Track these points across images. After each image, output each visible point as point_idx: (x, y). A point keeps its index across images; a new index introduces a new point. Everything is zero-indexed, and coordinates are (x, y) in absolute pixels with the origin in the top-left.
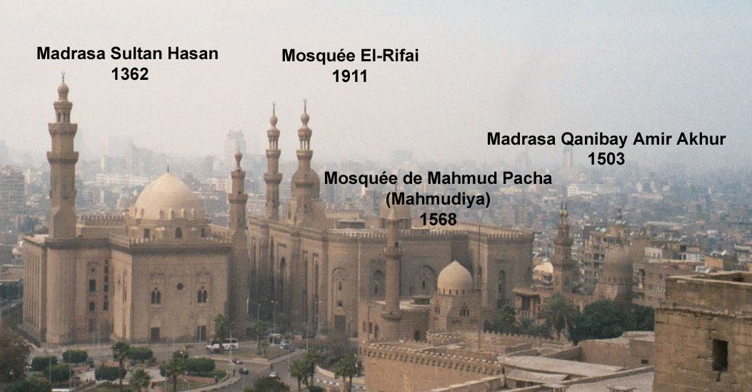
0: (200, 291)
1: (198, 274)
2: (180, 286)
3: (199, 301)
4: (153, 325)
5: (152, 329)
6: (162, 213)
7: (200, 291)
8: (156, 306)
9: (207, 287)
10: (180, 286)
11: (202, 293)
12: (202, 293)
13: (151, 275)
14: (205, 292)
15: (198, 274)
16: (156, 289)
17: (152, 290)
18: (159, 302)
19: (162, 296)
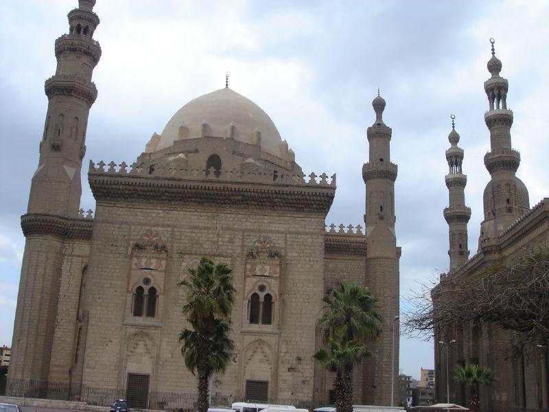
1: (251, 255)
3: (253, 320)
4: (133, 368)
5: (131, 376)
6: (183, 129)
7: (255, 296)
8: (142, 320)
9: (273, 287)
11: (262, 299)
12: (262, 299)
13: (137, 246)
14: (268, 297)
15: (251, 255)
16: (147, 281)
17: (137, 280)
18: (151, 313)
19: (161, 300)
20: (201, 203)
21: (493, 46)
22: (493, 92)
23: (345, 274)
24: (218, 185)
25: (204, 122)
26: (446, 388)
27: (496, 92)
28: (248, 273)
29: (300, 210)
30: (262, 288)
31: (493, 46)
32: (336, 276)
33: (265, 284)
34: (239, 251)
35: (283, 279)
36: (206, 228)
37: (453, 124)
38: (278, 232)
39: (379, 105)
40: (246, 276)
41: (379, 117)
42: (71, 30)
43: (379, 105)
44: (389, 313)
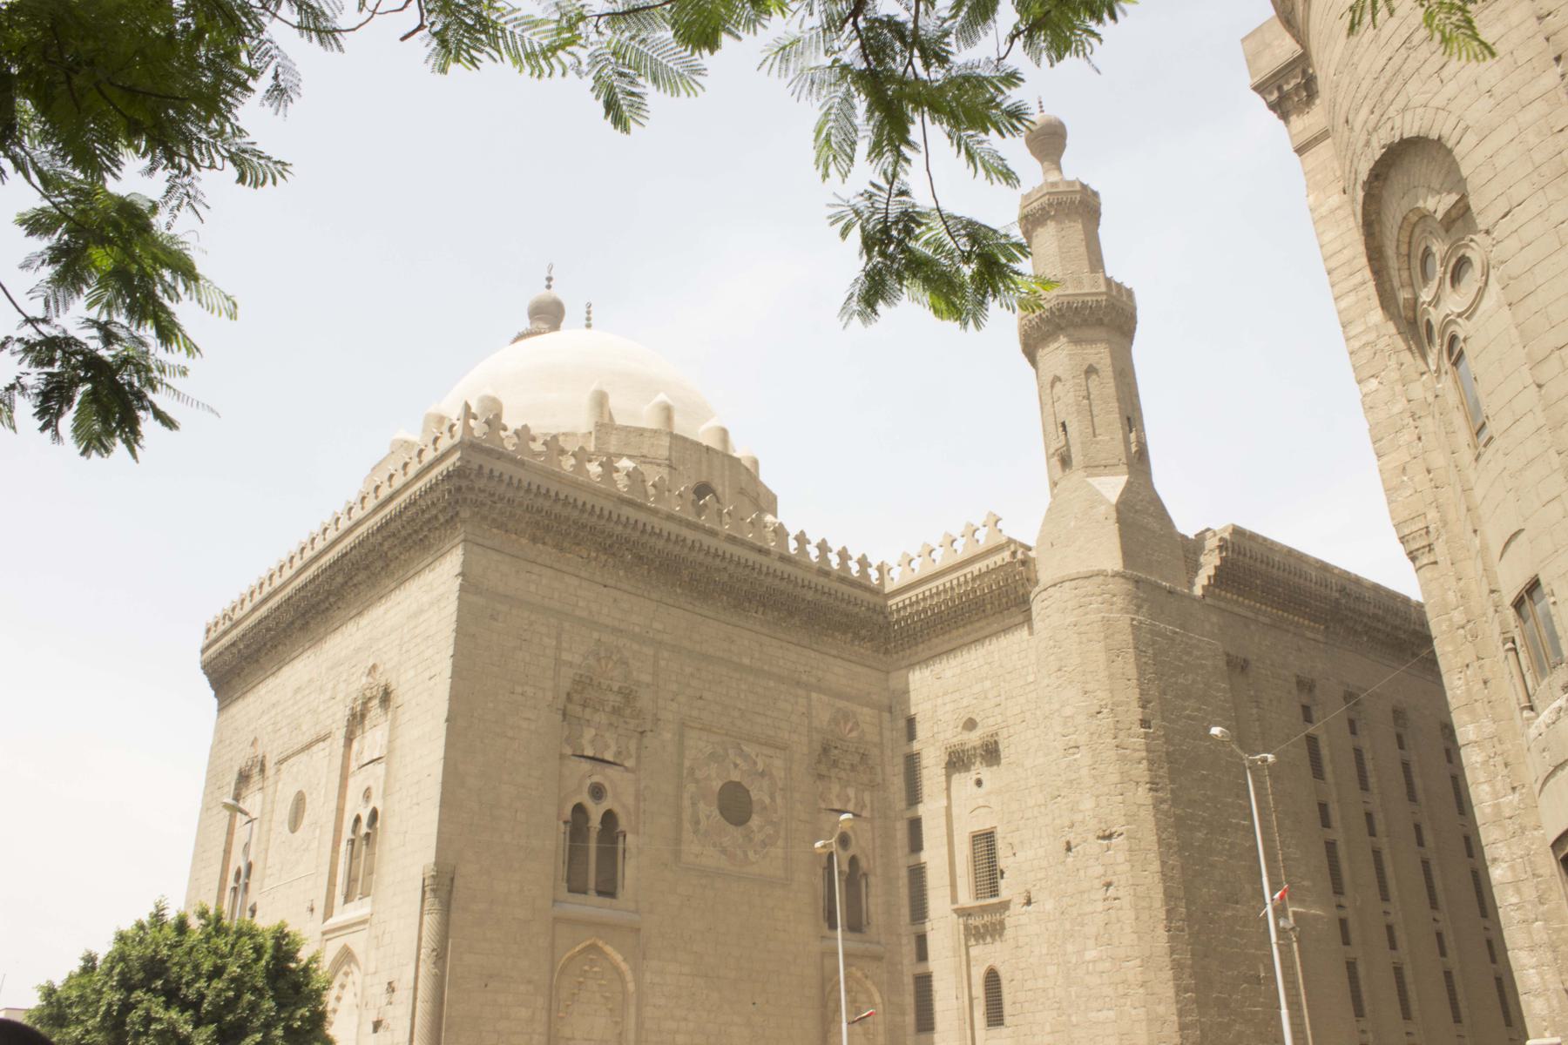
20: (305, 627)
23: (988, 684)
26: (1312, 1028)
32: (965, 703)
44: (1084, 772)
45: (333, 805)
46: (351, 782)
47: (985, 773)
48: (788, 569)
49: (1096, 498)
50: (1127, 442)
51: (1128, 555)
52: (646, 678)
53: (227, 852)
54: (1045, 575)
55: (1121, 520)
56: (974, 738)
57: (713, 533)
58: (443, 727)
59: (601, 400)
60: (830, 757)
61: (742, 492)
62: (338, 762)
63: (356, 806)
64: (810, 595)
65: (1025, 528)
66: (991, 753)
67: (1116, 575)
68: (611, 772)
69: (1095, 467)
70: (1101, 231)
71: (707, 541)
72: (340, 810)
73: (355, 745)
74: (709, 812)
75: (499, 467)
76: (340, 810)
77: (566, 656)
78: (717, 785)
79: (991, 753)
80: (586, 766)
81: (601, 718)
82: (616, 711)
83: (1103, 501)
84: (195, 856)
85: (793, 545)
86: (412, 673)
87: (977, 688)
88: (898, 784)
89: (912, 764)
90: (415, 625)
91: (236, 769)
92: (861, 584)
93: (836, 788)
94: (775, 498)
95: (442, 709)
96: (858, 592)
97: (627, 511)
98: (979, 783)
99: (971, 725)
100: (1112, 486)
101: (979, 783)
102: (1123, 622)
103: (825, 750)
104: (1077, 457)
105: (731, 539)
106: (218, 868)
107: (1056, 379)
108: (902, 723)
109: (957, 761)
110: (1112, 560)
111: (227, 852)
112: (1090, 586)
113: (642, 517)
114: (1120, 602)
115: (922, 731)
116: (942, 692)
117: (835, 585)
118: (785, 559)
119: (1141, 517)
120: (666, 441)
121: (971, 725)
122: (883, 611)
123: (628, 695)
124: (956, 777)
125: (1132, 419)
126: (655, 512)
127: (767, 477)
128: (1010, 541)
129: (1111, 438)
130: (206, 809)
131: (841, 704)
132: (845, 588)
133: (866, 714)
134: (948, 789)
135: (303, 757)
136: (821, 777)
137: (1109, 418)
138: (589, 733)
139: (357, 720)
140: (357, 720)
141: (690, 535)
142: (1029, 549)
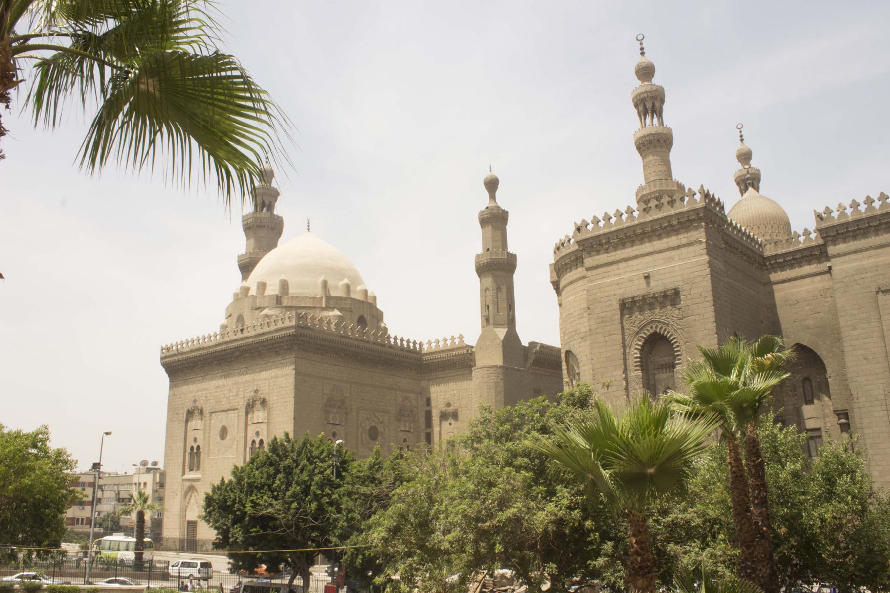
0: (253, 442)
2: (224, 433)
10: (224, 433)
17: (191, 442)
18: (198, 469)
20: (219, 364)
21: (641, 44)
22: (645, 106)
24: (224, 347)
25: (283, 277)
27: (649, 105)
28: (249, 422)
29: (277, 354)
30: (257, 434)
31: (641, 44)
33: (259, 430)
34: (241, 403)
35: (268, 424)
36: (224, 386)
37: (741, 136)
38: (265, 379)
39: (492, 185)
40: (246, 425)
41: (492, 196)
42: (256, 206)
43: (492, 185)
45: (243, 435)
46: (249, 427)
47: (453, 421)
48: (391, 350)
49: (496, 337)
50: (509, 315)
51: (505, 358)
52: (348, 395)
53: (186, 439)
54: (479, 362)
55: (504, 346)
56: (451, 409)
57: (368, 342)
58: (292, 421)
59: (325, 284)
60: (402, 413)
61: (373, 316)
62: (244, 420)
63: (251, 436)
64: (397, 358)
65: (472, 340)
66: (455, 415)
67: (501, 367)
68: (338, 427)
69: (497, 324)
70: (508, 227)
71: (367, 346)
72: (246, 437)
73: (250, 416)
74: (366, 437)
75: (306, 332)
76: (246, 437)
77: (325, 392)
78: (368, 428)
79: (455, 415)
80: (331, 426)
81: (335, 410)
82: (339, 407)
83: (499, 338)
84: (167, 438)
85: (392, 340)
86: (275, 398)
87: (452, 393)
88: (422, 420)
89: (428, 415)
90: (278, 382)
91: (186, 409)
92: (414, 352)
93: (403, 423)
94: (381, 314)
95: (292, 415)
96: (413, 355)
97: (343, 340)
98: (450, 424)
99: (449, 405)
100: (502, 332)
101: (450, 424)
102: (502, 383)
103: (400, 411)
104: (491, 320)
105: (374, 343)
106: (182, 445)
107: (486, 289)
108: (425, 399)
109: (444, 416)
110: (499, 362)
111: (186, 439)
112: (492, 371)
113: (348, 341)
114: (501, 376)
115: (433, 403)
116: (441, 394)
117: (405, 353)
118: (390, 347)
119: (512, 338)
120: (349, 302)
121: (449, 405)
122: (421, 360)
123: (342, 402)
124: (443, 422)
125: (511, 307)
126: (351, 338)
127: (379, 306)
128: (467, 346)
129: (503, 314)
130: (170, 420)
131: (405, 394)
132: (408, 354)
133: (413, 396)
134: (440, 425)
135: (224, 413)
136: (399, 420)
137: (504, 306)
138: (332, 415)
139: (250, 407)
140: (250, 407)
141: (361, 344)
142: (472, 347)
